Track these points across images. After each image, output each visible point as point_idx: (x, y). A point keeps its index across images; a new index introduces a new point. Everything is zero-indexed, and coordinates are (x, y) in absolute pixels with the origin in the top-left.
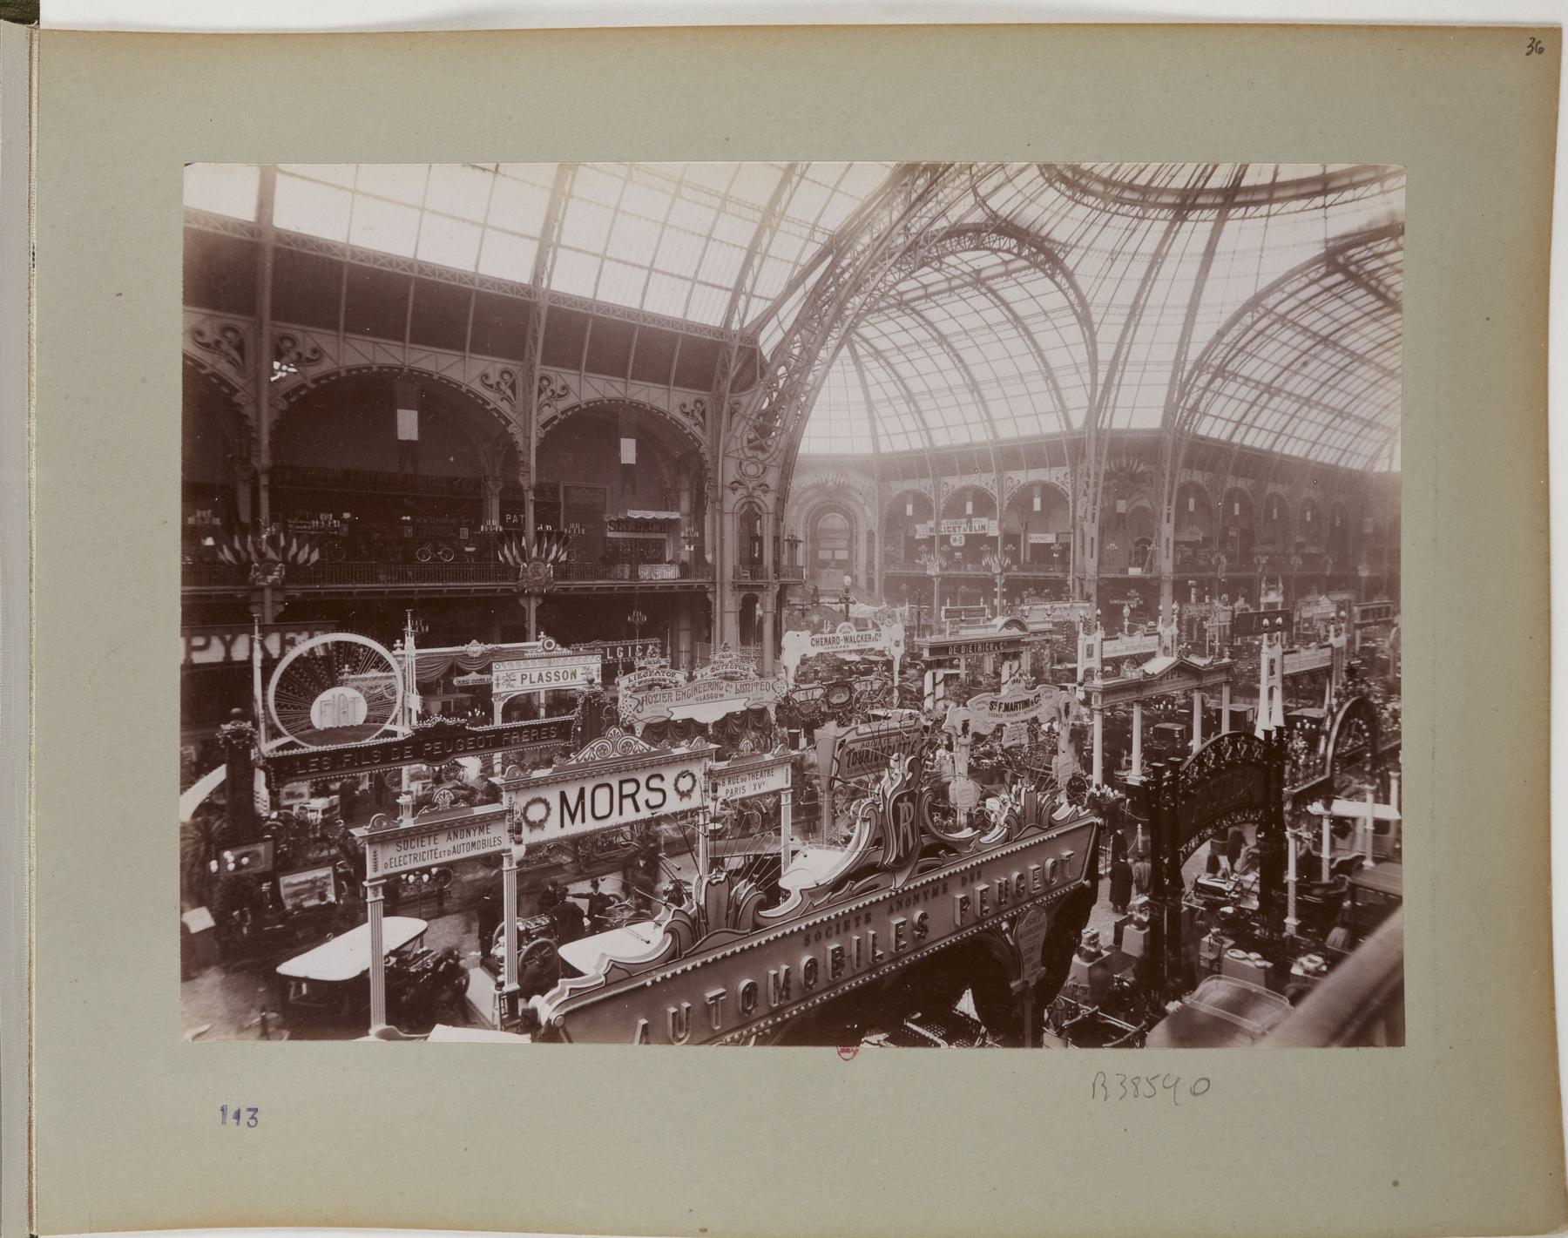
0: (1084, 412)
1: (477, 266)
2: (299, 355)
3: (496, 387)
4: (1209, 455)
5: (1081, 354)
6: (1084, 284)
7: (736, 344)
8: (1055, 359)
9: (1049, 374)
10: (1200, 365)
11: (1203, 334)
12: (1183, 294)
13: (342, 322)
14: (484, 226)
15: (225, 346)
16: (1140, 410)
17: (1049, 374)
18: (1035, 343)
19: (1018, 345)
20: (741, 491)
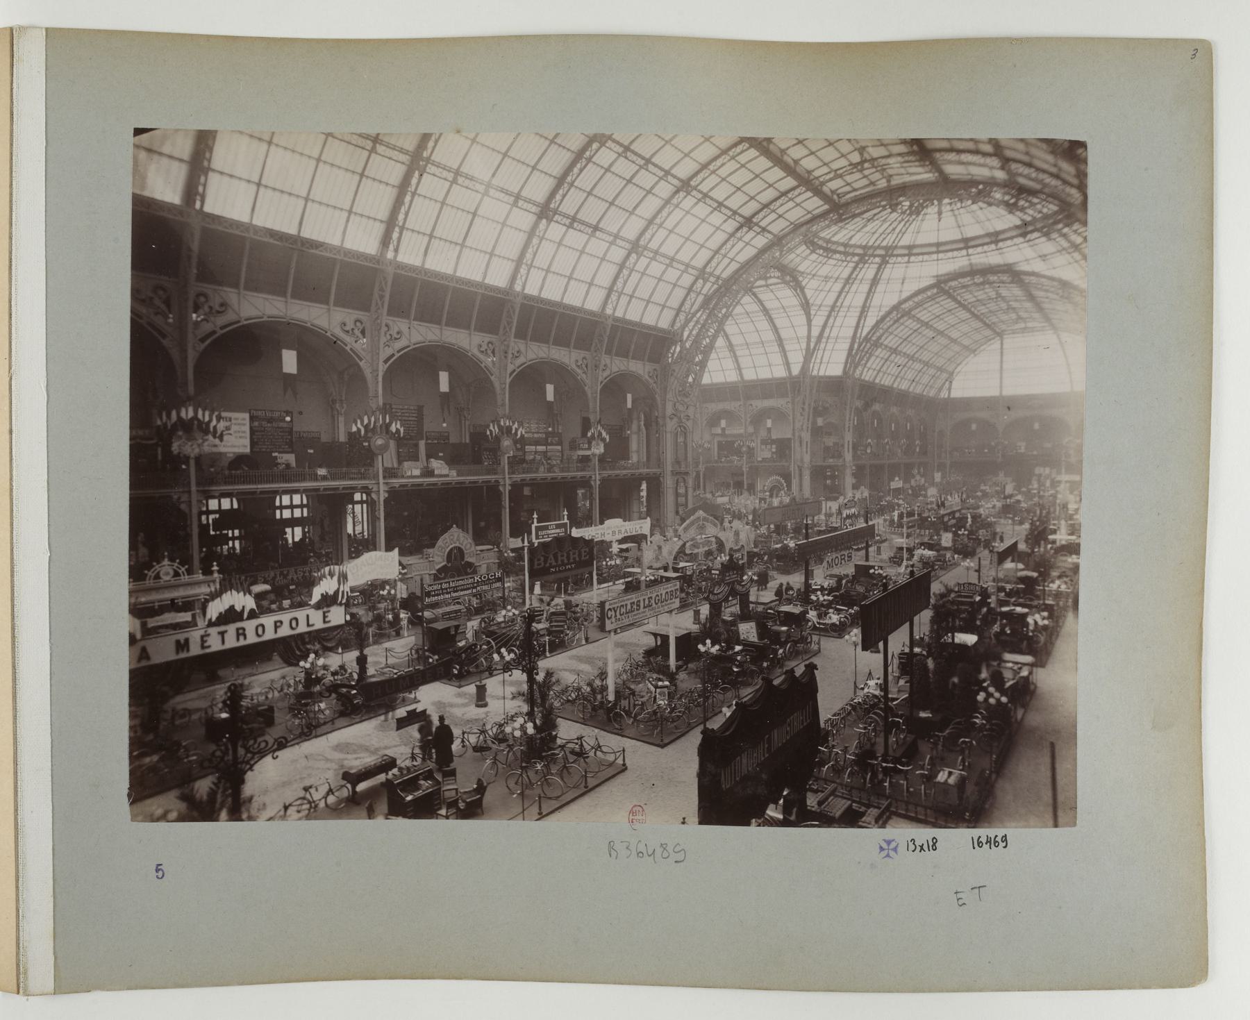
0: (800, 365)
1: (455, 271)
2: (211, 308)
3: (484, 352)
4: (872, 393)
5: (803, 332)
6: (809, 293)
7: (610, 322)
8: (783, 334)
9: (780, 342)
10: (867, 339)
11: (870, 321)
12: (859, 300)
13: (243, 280)
14: (431, 236)
15: (157, 302)
16: (832, 364)
17: (780, 342)
18: (775, 326)
19: (764, 324)
20: (675, 419)
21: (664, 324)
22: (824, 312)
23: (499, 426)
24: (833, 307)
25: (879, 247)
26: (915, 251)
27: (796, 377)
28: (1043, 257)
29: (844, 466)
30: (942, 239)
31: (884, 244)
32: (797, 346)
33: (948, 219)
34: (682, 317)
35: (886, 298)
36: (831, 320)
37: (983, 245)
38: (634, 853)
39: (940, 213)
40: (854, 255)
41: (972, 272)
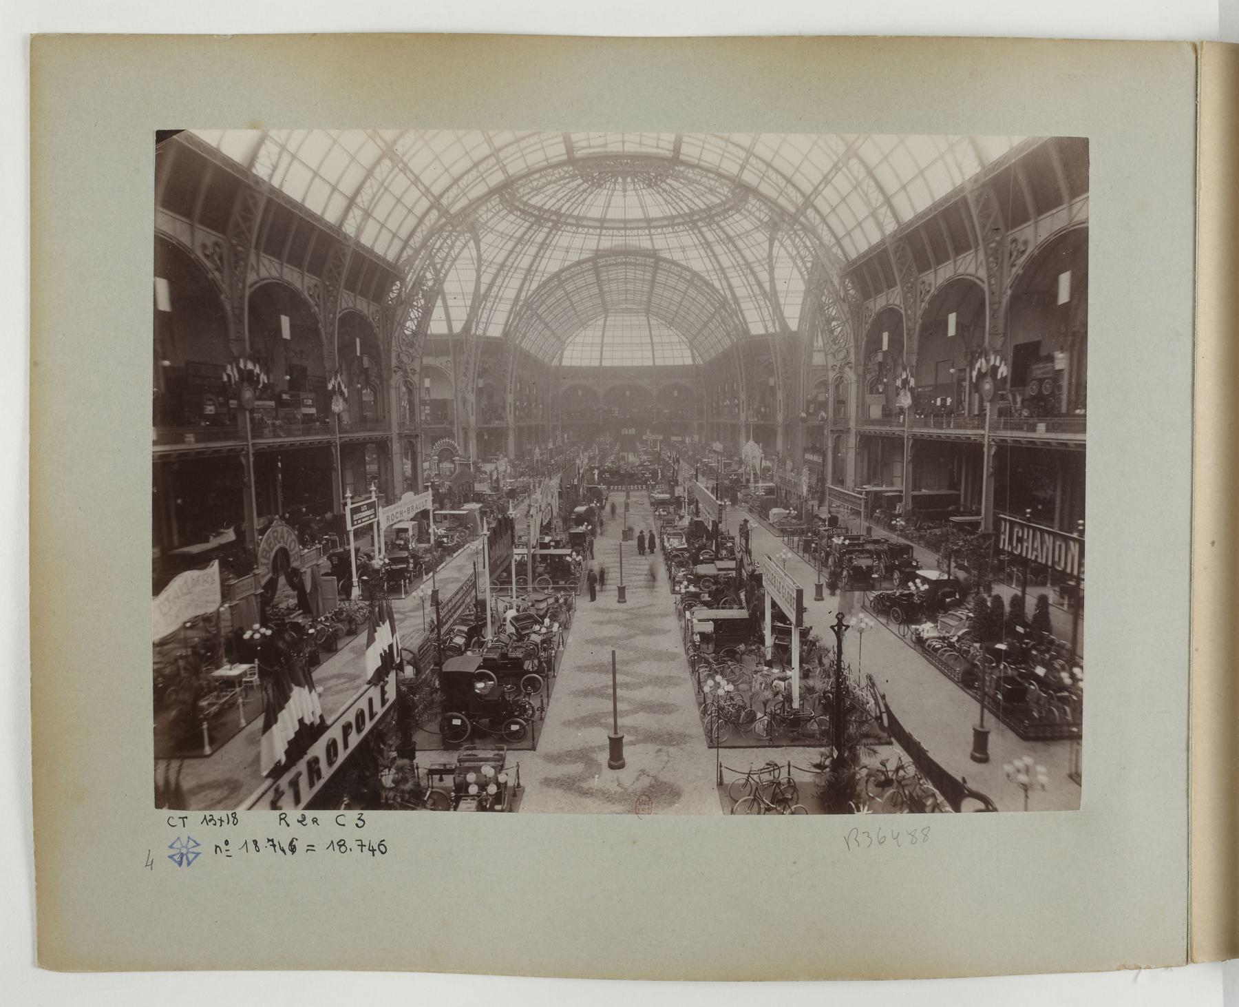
6: (483, 246)
10: (526, 300)
12: (525, 262)
20: (400, 373)
21: (391, 257)
22: (493, 270)
23: (239, 370)
24: (502, 266)
25: (570, 216)
26: (585, 223)
27: (457, 335)
28: (683, 249)
29: (507, 428)
30: (629, 216)
31: (575, 213)
32: (461, 303)
33: (632, 198)
34: (409, 251)
35: (551, 264)
36: (500, 280)
37: (638, 228)
38: (875, 841)
39: (625, 190)
40: (532, 215)
41: (626, 252)
